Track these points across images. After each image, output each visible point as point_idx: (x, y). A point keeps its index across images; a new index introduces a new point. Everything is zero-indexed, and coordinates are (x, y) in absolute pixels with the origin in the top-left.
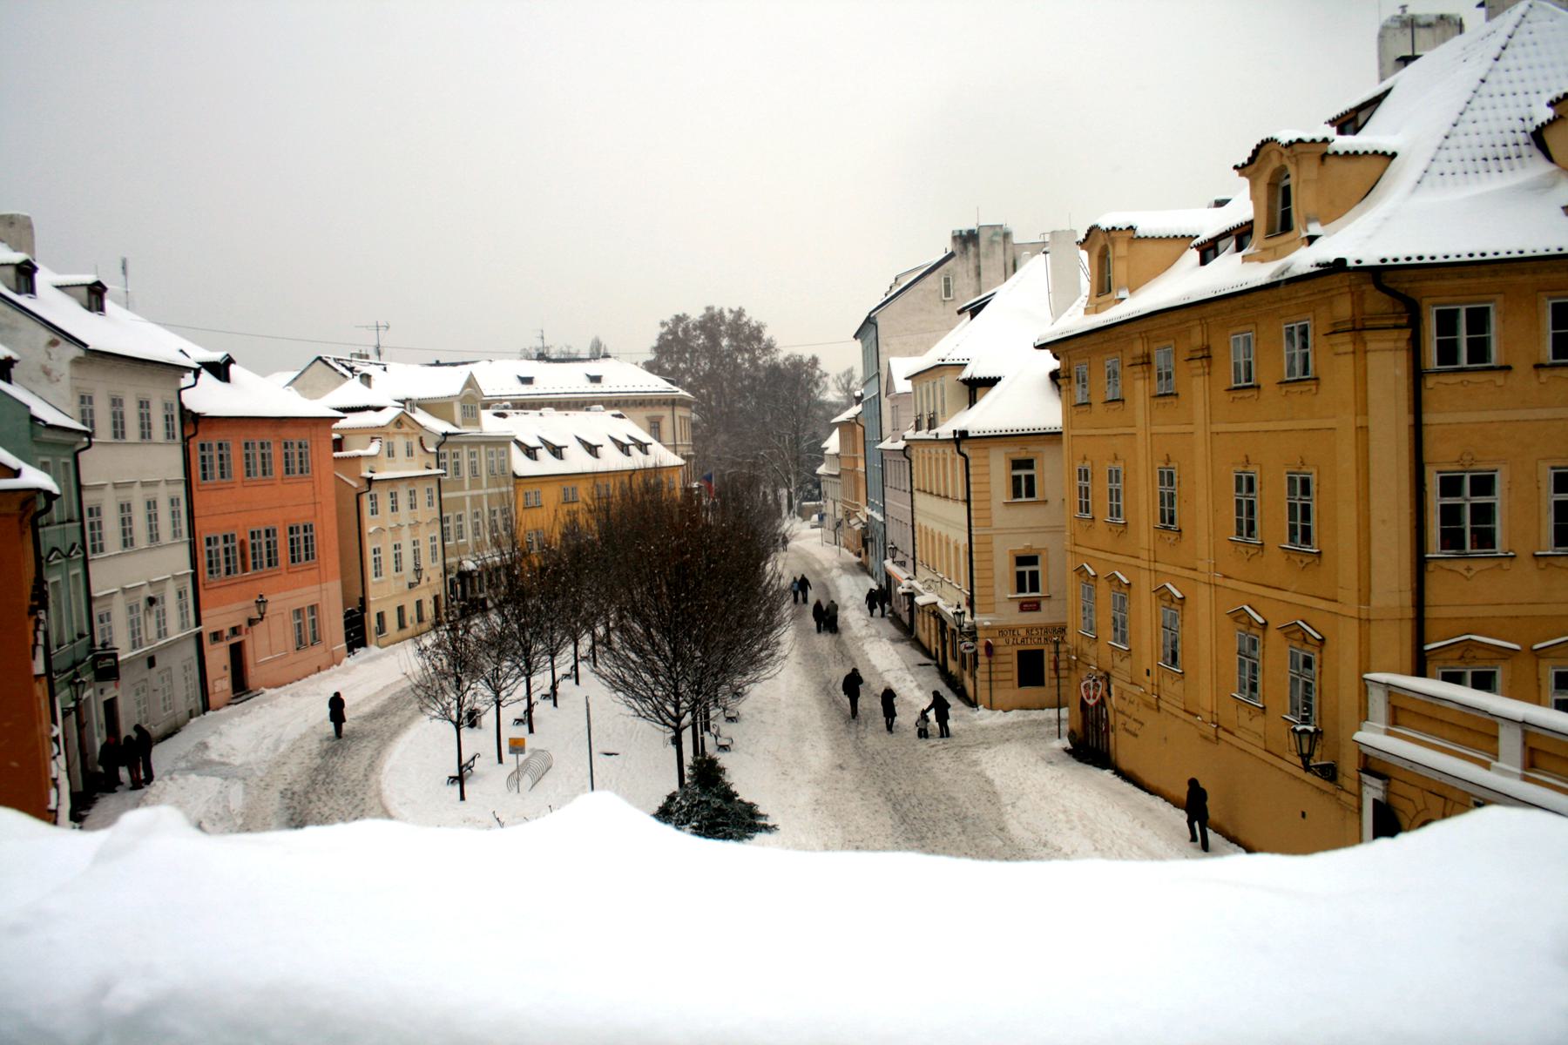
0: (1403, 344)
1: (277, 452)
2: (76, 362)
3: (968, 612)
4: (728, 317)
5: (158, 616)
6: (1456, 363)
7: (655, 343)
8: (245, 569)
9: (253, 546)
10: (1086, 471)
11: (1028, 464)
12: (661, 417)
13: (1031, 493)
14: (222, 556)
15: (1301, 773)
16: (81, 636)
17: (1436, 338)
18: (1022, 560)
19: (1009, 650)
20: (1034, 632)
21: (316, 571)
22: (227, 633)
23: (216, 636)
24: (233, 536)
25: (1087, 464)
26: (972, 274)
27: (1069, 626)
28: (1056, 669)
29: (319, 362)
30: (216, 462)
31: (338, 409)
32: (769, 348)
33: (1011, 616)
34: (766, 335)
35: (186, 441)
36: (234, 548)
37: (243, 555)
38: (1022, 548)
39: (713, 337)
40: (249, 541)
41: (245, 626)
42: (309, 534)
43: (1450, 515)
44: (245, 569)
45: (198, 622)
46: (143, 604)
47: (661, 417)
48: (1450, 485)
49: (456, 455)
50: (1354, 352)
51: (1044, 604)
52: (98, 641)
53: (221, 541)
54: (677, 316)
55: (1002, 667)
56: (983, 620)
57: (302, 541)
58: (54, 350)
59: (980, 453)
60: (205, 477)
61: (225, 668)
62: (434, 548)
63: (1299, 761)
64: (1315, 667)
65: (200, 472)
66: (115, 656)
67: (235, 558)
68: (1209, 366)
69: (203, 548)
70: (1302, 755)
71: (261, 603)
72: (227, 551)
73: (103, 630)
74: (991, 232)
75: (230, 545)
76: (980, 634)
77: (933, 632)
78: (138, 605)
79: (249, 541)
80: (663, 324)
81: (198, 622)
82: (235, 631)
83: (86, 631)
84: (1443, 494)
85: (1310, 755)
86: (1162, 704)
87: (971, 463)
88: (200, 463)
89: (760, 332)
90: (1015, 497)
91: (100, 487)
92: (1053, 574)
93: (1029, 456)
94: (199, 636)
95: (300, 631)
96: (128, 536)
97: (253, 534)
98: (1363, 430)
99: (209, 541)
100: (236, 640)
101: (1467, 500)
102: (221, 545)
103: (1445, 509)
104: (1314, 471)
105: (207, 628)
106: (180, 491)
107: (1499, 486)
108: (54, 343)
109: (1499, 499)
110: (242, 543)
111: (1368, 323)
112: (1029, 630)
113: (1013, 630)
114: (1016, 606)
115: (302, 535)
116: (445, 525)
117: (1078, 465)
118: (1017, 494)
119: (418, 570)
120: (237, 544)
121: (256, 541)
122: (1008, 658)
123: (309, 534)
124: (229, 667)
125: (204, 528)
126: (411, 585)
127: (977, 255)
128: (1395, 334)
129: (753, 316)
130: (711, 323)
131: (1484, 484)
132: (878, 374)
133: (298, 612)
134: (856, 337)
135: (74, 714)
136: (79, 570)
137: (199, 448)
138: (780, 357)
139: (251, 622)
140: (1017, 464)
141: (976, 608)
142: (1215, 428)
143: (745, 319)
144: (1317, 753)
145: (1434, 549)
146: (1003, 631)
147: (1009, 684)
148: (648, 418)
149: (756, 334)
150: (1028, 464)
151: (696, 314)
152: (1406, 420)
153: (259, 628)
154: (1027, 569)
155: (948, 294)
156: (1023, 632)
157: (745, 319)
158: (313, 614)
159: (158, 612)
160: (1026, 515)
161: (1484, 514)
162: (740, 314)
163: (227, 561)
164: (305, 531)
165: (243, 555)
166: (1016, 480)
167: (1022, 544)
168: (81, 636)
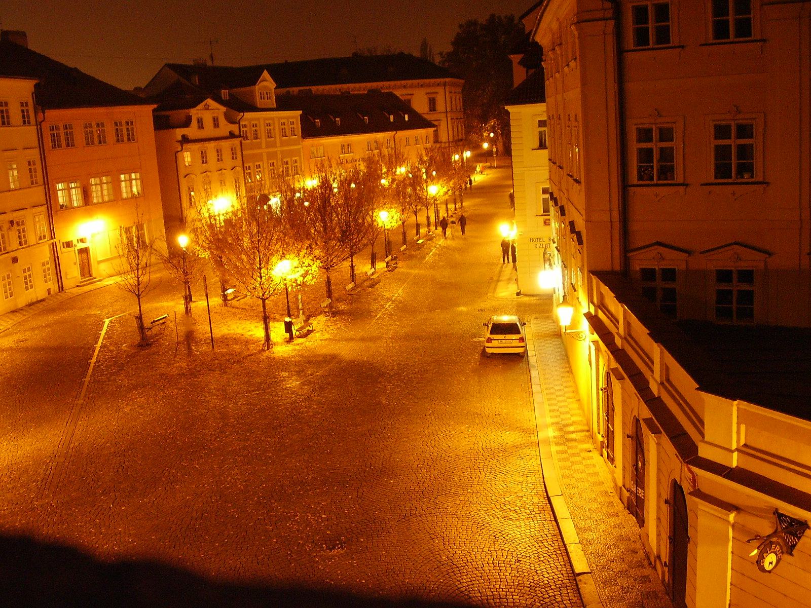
6: (669, 43)
35: (39, 124)
43: (645, 156)
48: (645, 135)
61: (75, 264)
84: (639, 140)
100: (81, 246)
101: (655, 146)
103: (640, 151)
107: (678, 135)
109: (677, 144)
131: (666, 135)
152: (613, 88)
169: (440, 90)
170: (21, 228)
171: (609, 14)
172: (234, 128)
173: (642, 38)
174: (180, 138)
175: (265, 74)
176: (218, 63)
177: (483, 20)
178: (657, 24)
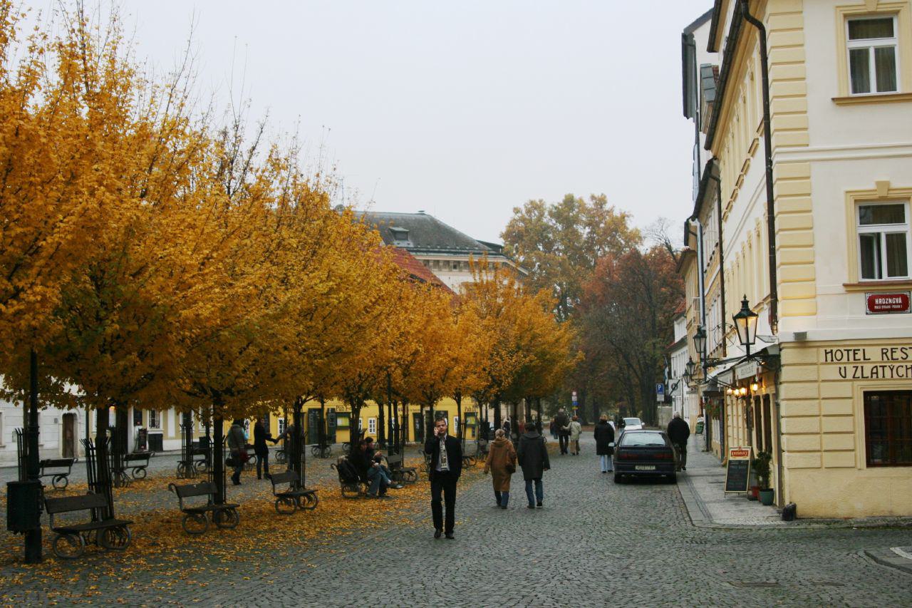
7: (504, 231)
20: (898, 355)
34: (631, 225)
38: (872, 186)
39: (569, 222)
54: (532, 202)
56: (788, 327)
77: (741, 430)
80: (516, 211)
90: (855, 91)
112: (889, 349)
114: (861, 300)
129: (616, 205)
130: (568, 211)
138: (645, 248)
143: (607, 207)
147: (847, 459)
149: (618, 224)
151: (553, 199)
154: (884, 229)
156: (874, 354)
162: (601, 202)
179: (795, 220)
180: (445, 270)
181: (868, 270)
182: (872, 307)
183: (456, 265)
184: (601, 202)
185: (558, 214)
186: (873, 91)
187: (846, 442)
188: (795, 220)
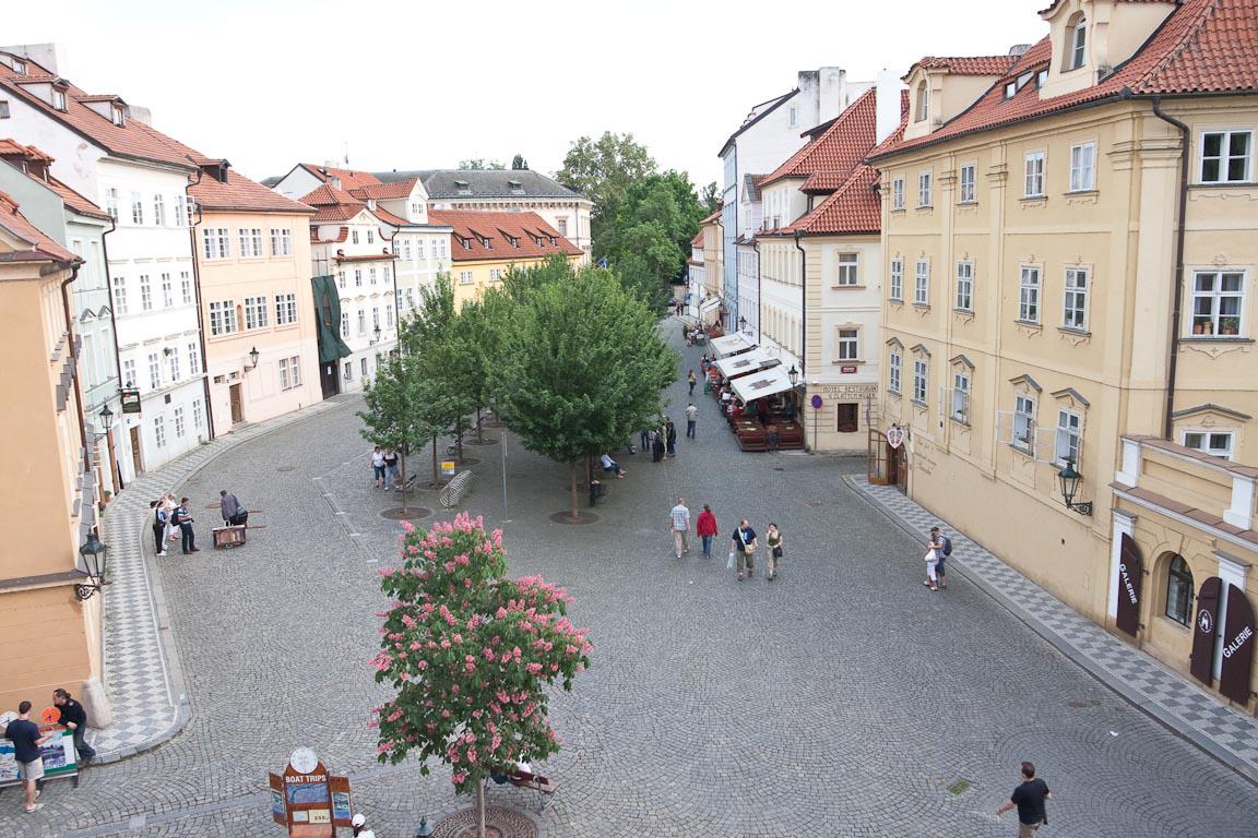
0: (1174, 163)
1: (265, 237)
2: (103, 160)
3: (800, 371)
4: (622, 139)
5: (172, 363)
6: (1217, 179)
8: (240, 325)
9: (248, 309)
10: (899, 263)
11: (853, 257)
12: (567, 217)
13: (853, 281)
14: (223, 318)
15: (1064, 509)
16: (110, 378)
17: (1203, 158)
18: (843, 333)
19: (831, 402)
21: (297, 330)
22: (228, 377)
23: (217, 379)
24: (231, 302)
25: (900, 259)
26: (813, 106)
27: (880, 386)
28: (868, 418)
29: (299, 168)
30: (218, 244)
31: (313, 206)
32: (650, 165)
33: (834, 376)
34: (649, 155)
36: (232, 311)
37: (240, 317)
39: (608, 155)
40: (244, 307)
41: (241, 371)
42: (291, 302)
43: (1205, 305)
44: (240, 325)
45: (205, 370)
46: (161, 354)
47: (567, 217)
48: (1206, 282)
49: (407, 242)
50: (1131, 169)
51: (859, 368)
52: (124, 383)
53: (222, 305)
55: (825, 416)
56: (811, 379)
57: (286, 306)
58: (82, 152)
59: (814, 247)
60: (208, 256)
62: (389, 314)
63: (1063, 500)
64: (1080, 425)
65: (205, 252)
66: (137, 394)
67: (233, 319)
68: (1005, 179)
69: (207, 311)
70: (1065, 495)
71: (254, 352)
72: (226, 313)
73: (128, 374)
74: (830, 72)
75: (228, 309)
76: (809, 389)
78: (155, 355)
79: (244, 307)
81: (205, 370)
82: (233, 375)
83: (115, 374)
85: (1071, 496)
86: (951, 450)
87: (806, 256)
88: (204, 245)
89: (644, 151)
91: (124, 261)
92: (871, 347)
93: (854, 251)
94: (206, 379)
95: (285, 376)
96: (147, 301)
97: (247, 300)
98: (1134, 234)
99: (212, 305)
101: (1217, 293)
102: (222, 309)
104: (1090, 268)
105: (211, 375)
106: (189, 267)
107: (1246, 282)
108: (85, 147)
109: (1244, 293)
110: (239, 306)
111: (1146, 145)
112: (848, 387)
113: (835, 387)
114: (838, 368)
115: (286, 302)
116: (399, 297)
117: (893, 259)
118: (842, 281)
119: (377, 330)
120: (235, 308)
121: (250, 306)
122: (830, 409)
123: (291, 302)
124: (229, 403)
125: (207, 300)
126: (371, 343)
127: (818, 92)
128: (1167, 154)
129: (639, 140)
130: (606, 145)
132: (736, 185)
133: (283, 362)
134: (719, 156)
135: (105, 437)
136: (109, 326)
137: (203, 233)
138: (659, 172)
139: (246, 369)
140: (843, 257)
141: (806, 368)
142: (1008, 231)
144: (1078, 493)
145: (1187, 329)
146: (826, 387)
148: (556, 217)
149: (642, 154)
150: (853, 257)
153: (251, 373)
154: (848, 340)
155: (793, 123)
156: (843, 389)
157: (632, 142)
158: (295, 363)
159: (172, 360)
160: (849, 298)
161: (1229, 305)
162: (629, 138)
163: (227, 321)
164: (289, 299)
165: (240, 317)
166: (842, 269)
167: (845, 321)
168: (110, 378)
169: (570, 212)
170: (174, 356)
171: (1176, 144)
172: (388, 245)
173: (1210, 171)
174: (335, 255)
175: (419, 181)
176: (352, 167)
177: (596, 139)
178: (1232, 157)
179: (812, 322)
180: (545, 209)
181: (842, 355)
182: (842, 371)
183: (552, 205)
184: (629, 138)
185: (601, 147)
186: (848, 284)
187: (830, 423)
188: (812, 322)
